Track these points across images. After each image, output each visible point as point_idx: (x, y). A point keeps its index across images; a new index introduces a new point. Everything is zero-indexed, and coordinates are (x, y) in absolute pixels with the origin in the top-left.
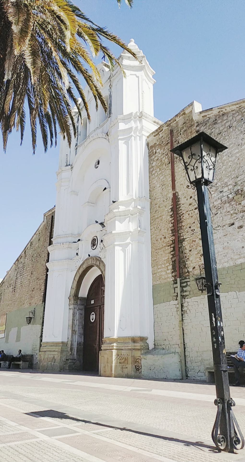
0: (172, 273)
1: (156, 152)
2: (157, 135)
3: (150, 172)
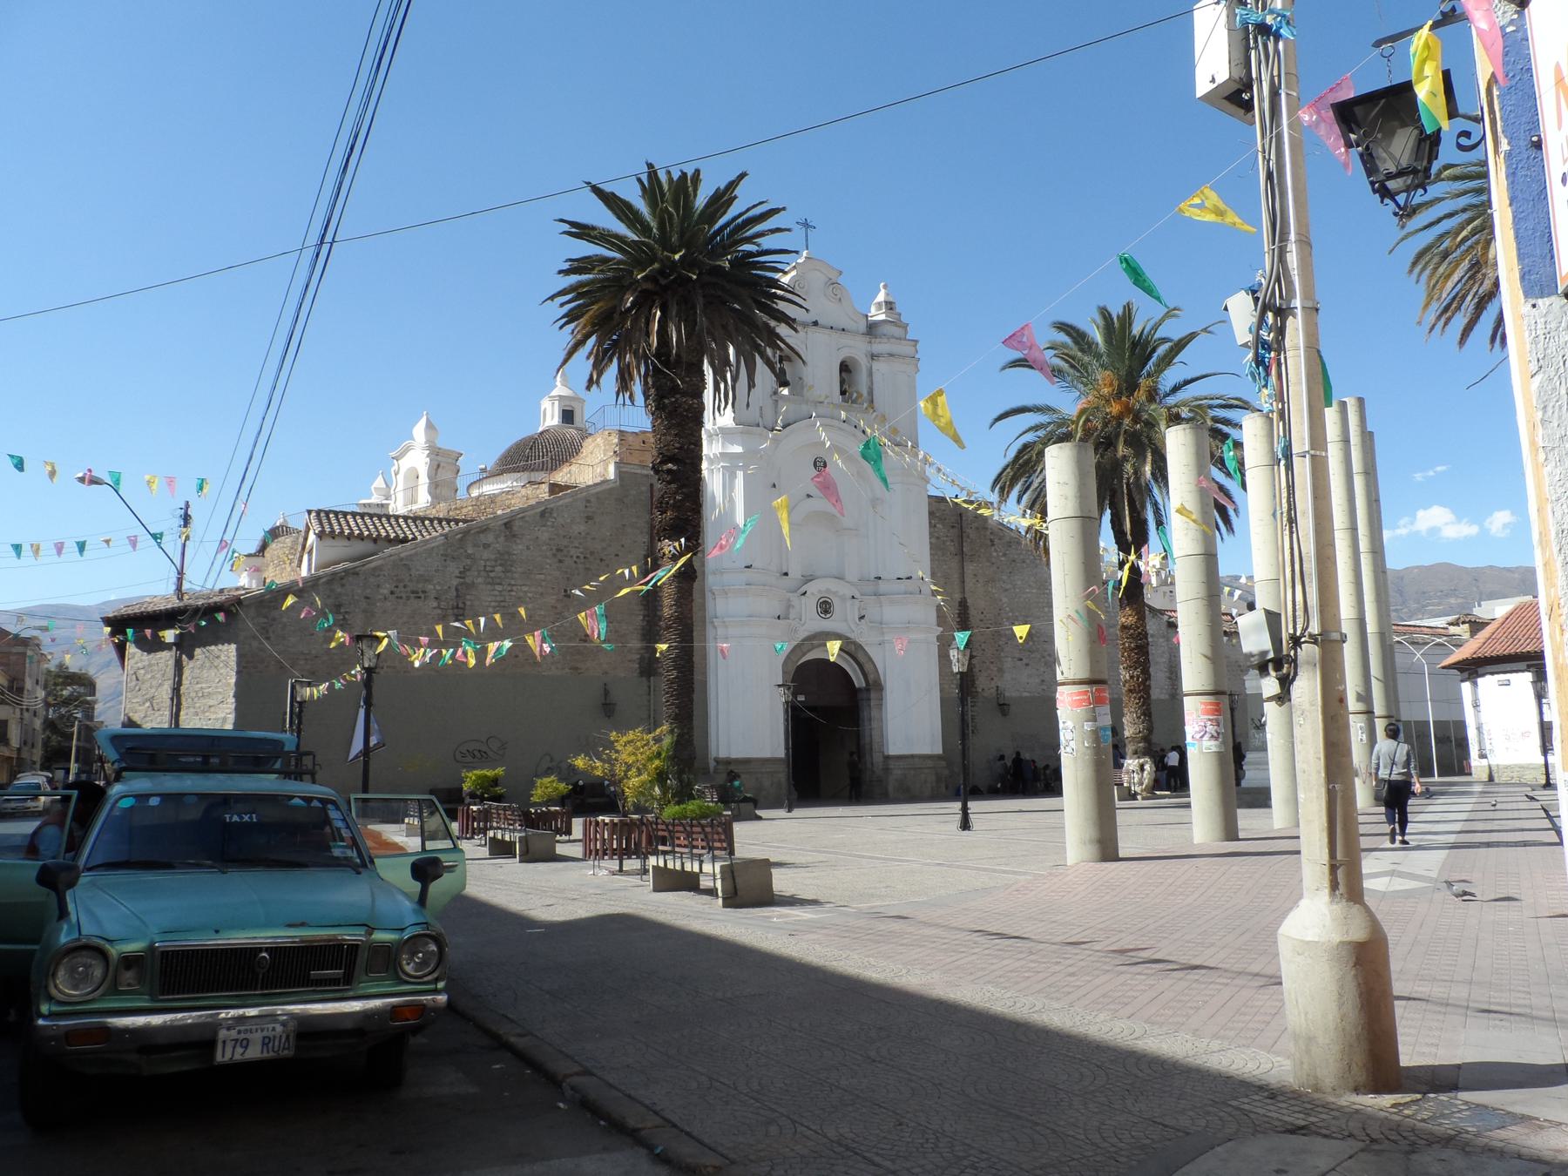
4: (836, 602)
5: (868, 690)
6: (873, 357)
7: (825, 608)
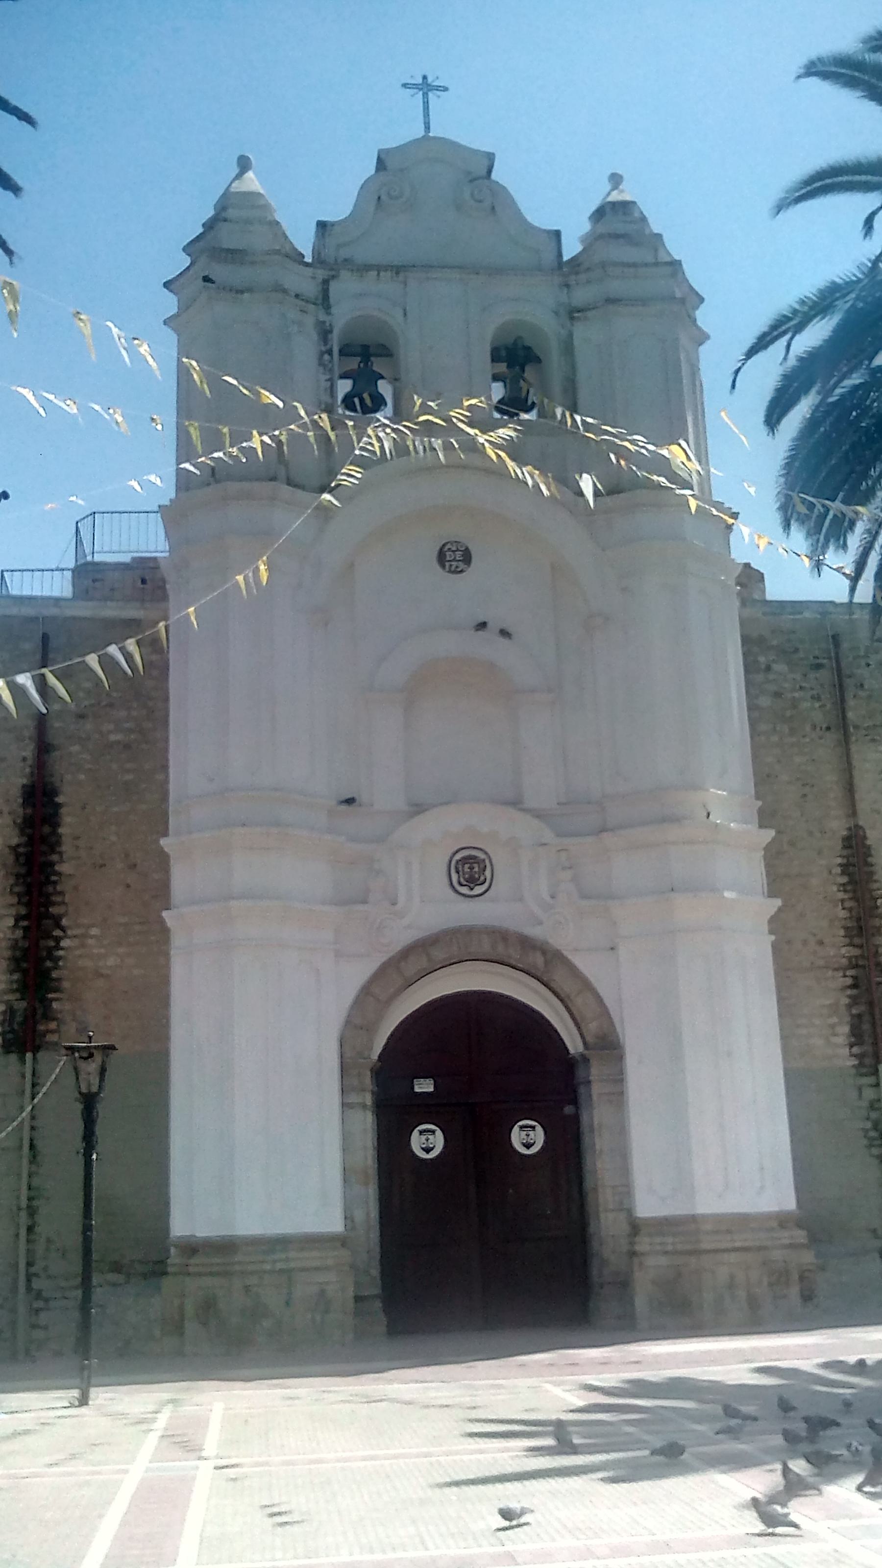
0: (851, 1046)
1: (768, 668)
2: (774, 614)
3: (753, 724)
4: (500, 859)
5: (585, 1059)
6: (574, 313)
7: (470, 872)
